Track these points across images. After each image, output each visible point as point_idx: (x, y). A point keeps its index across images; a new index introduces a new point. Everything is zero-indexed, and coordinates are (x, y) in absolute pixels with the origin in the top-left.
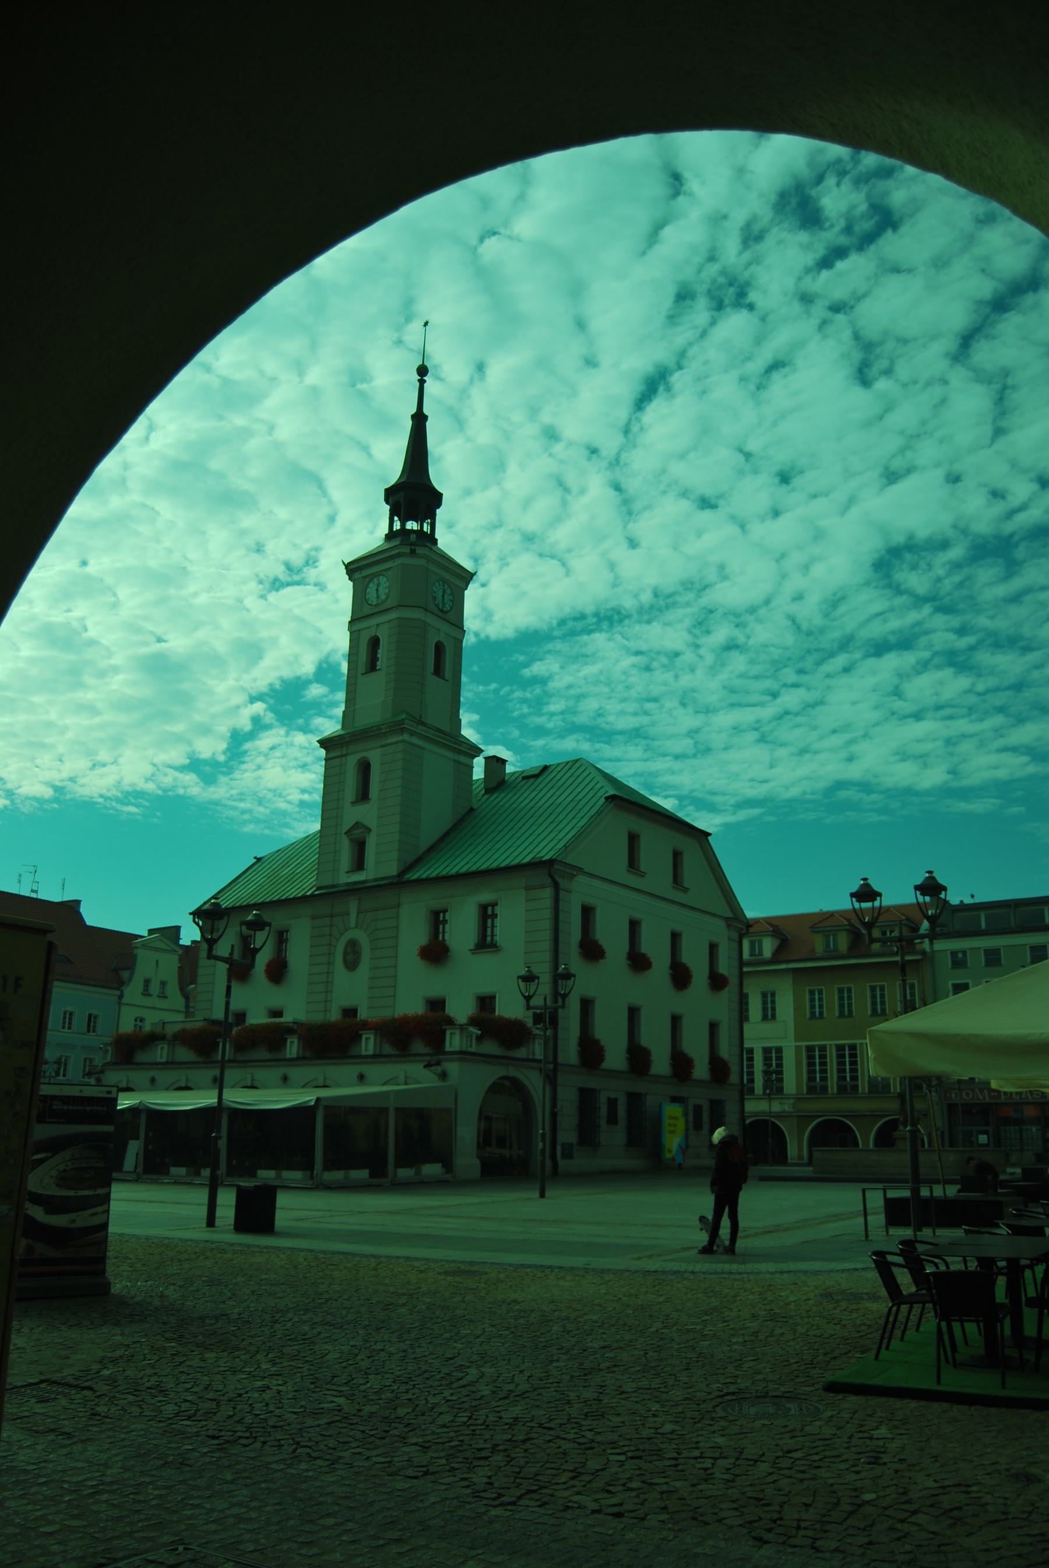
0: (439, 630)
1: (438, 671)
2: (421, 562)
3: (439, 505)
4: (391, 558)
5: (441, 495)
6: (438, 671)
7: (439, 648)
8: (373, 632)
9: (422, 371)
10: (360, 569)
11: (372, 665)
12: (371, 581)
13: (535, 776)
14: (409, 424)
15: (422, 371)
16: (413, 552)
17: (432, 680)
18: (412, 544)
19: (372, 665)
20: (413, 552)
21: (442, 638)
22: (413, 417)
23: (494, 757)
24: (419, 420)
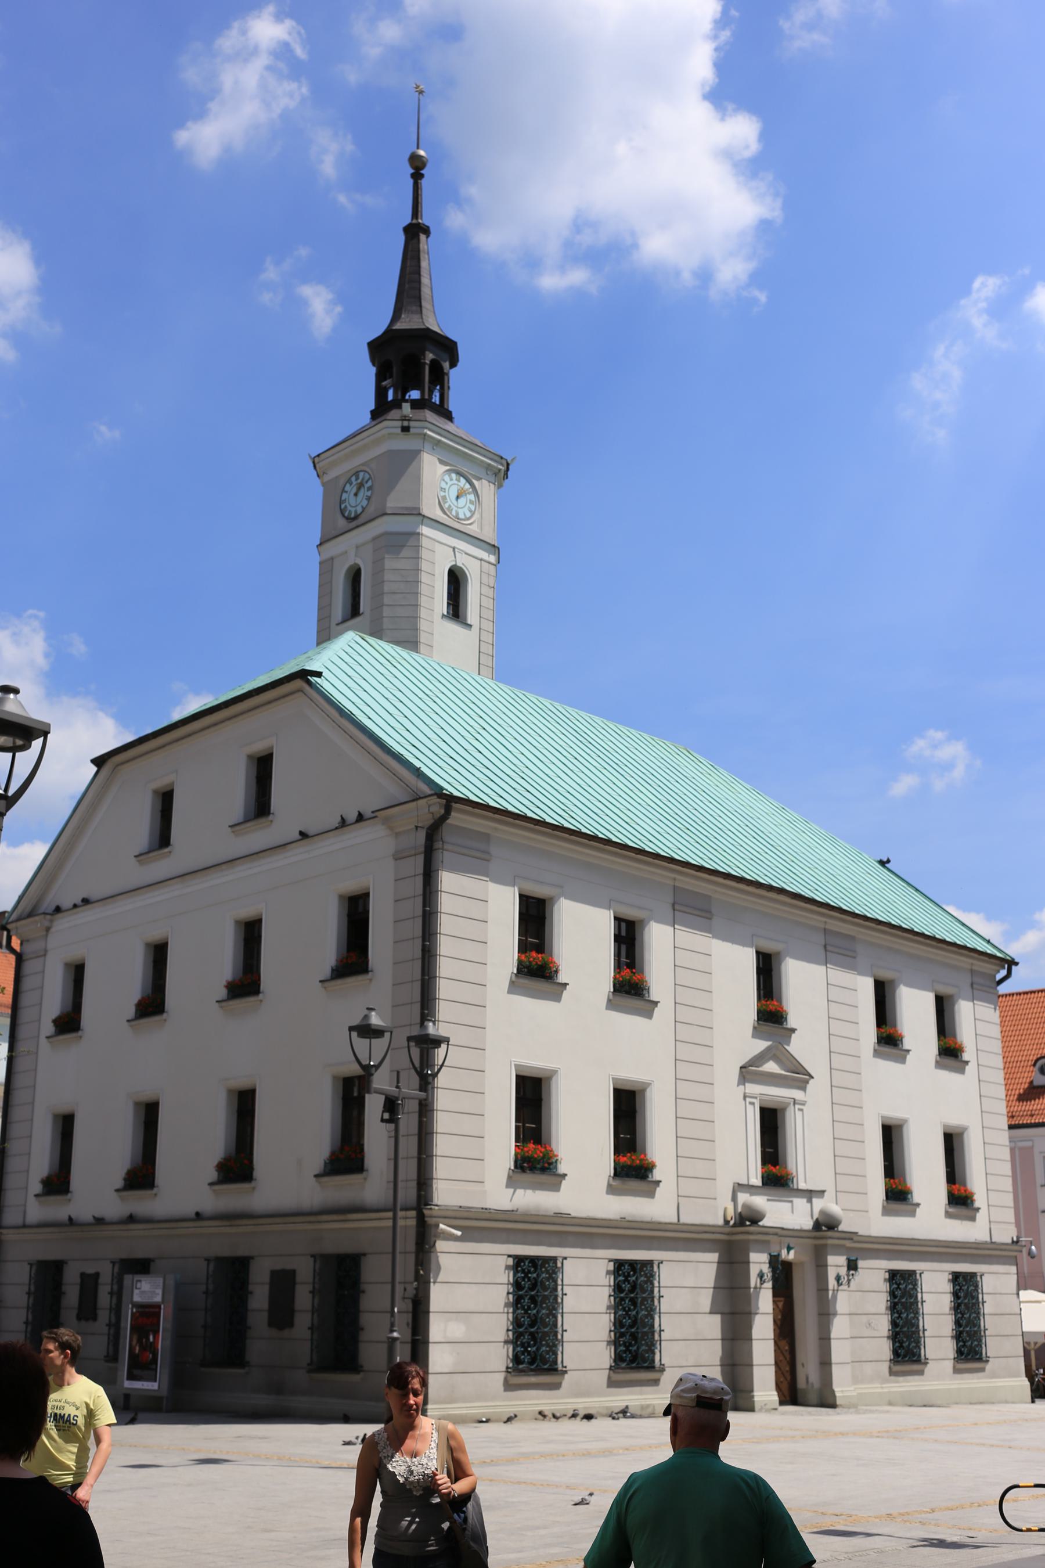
5: (455, 343)
8: (351, 560)
20: (405, 429)
21: (461, 561)
24: (415, 232)
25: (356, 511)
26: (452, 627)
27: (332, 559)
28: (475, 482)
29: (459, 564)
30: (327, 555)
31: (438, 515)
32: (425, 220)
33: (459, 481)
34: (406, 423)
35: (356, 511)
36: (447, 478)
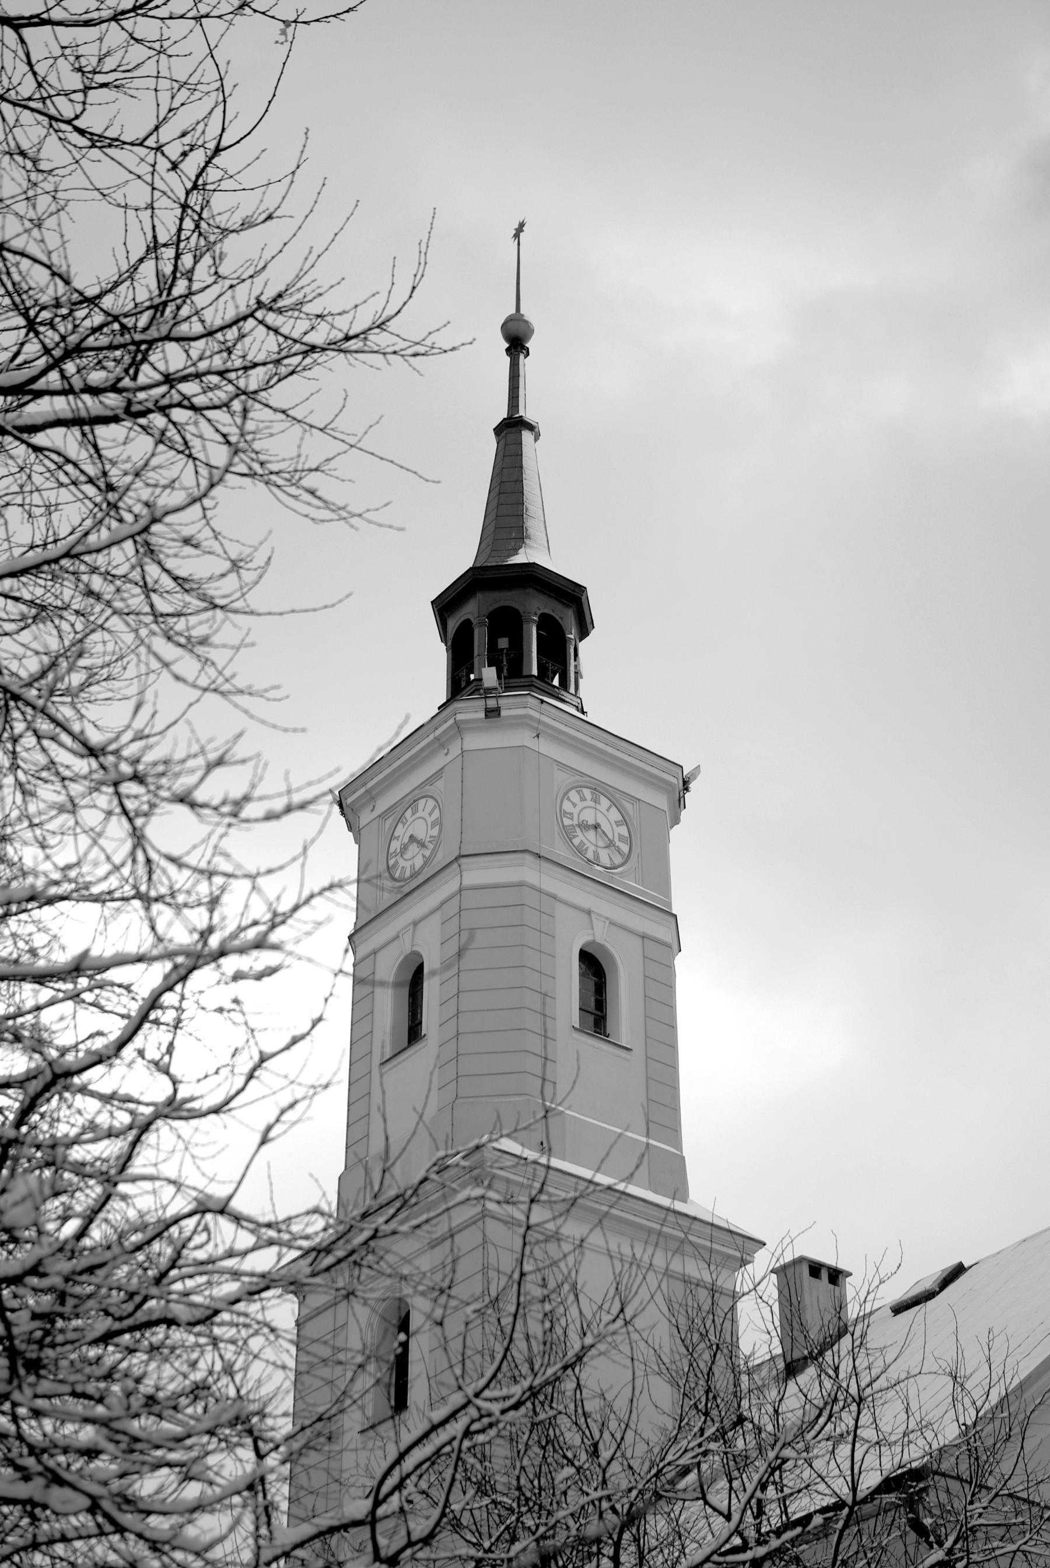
0: (589, 912)
1: (597, 1016)
4: (441, 744)
5: (582, 589)
6: (597, 1016)
7: (593, 966)
10: (371, 797)
12: (401, 819)
13: (929, 1296)
14: (486, 449)
20: (492, 713)
21: (601, 936)
22: (500, 430)
23: (801, 1260)
25: (413, 866)
26: (591, 1044)
27: (375, 952)
28: (628, 806)
29: (598, 940)
30: (364, 950)
31: (561, 851)
32: (528, 411)
33: (596, 801)
34: (492, 703)
35: (413, 866)
36: (574, 795)
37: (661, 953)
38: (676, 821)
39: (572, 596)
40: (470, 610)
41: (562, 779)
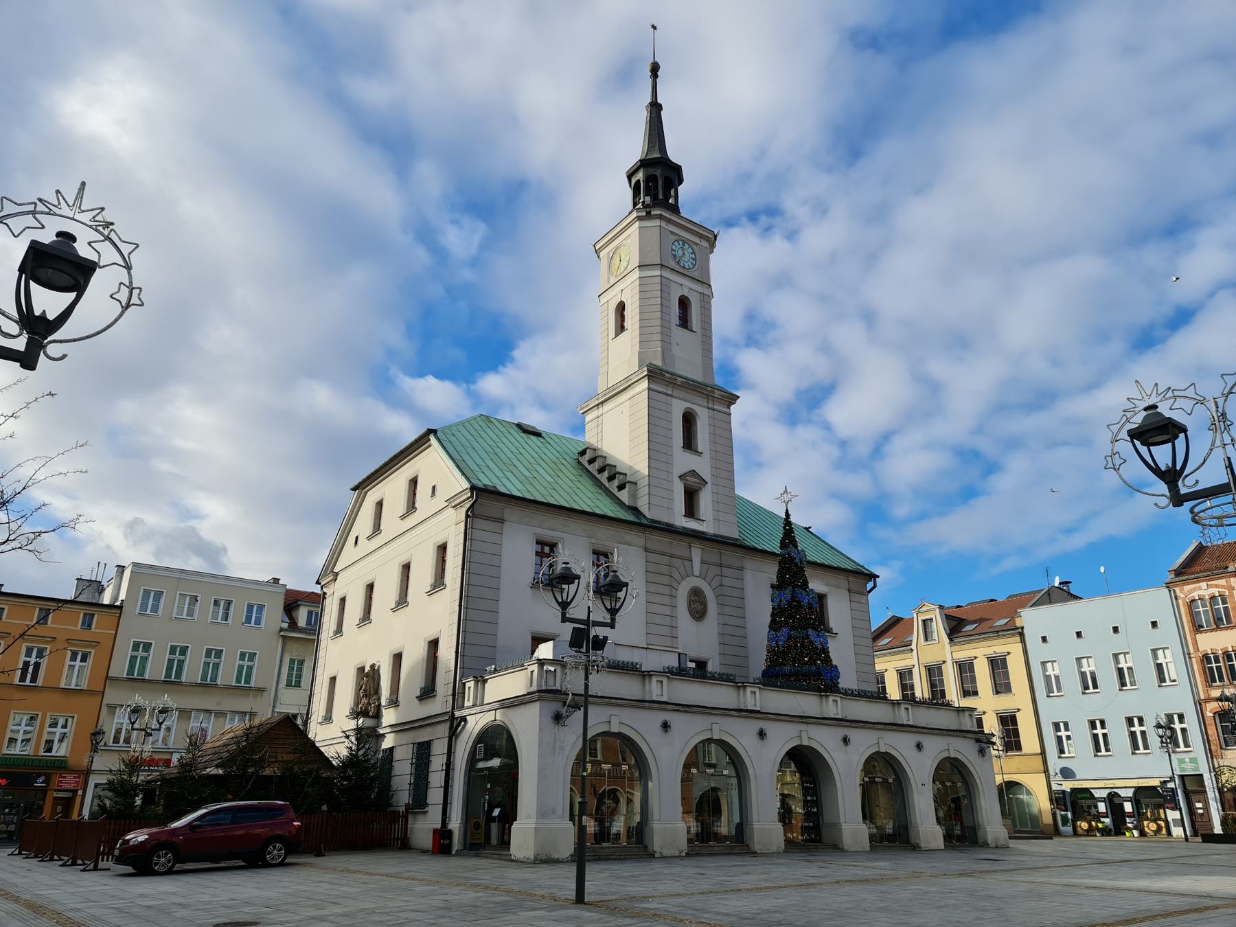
1: (684, 322)
2: (656, 223)
3: (681, 181)
6: (684, 322)
7: (684, 303)
9: (655, 69)
11: (621, 328)
14: (643, 116)
15: (655, 69)
16: (648, 213)
17: (679, 333)
18: (648, 206)
19: (621, 328)
20: (648, 213)
24: (655, 108)
31: (673, 264)
37: (706, 299)
38: (712, 252)
39: (677, 169)
40: (640, 176)
41: (673, 238)
